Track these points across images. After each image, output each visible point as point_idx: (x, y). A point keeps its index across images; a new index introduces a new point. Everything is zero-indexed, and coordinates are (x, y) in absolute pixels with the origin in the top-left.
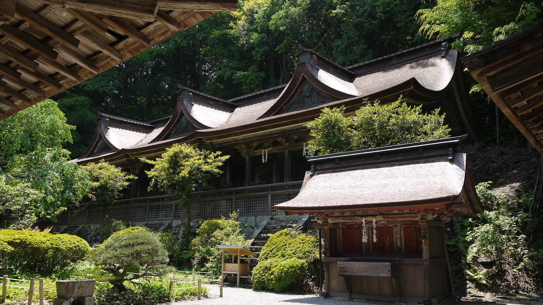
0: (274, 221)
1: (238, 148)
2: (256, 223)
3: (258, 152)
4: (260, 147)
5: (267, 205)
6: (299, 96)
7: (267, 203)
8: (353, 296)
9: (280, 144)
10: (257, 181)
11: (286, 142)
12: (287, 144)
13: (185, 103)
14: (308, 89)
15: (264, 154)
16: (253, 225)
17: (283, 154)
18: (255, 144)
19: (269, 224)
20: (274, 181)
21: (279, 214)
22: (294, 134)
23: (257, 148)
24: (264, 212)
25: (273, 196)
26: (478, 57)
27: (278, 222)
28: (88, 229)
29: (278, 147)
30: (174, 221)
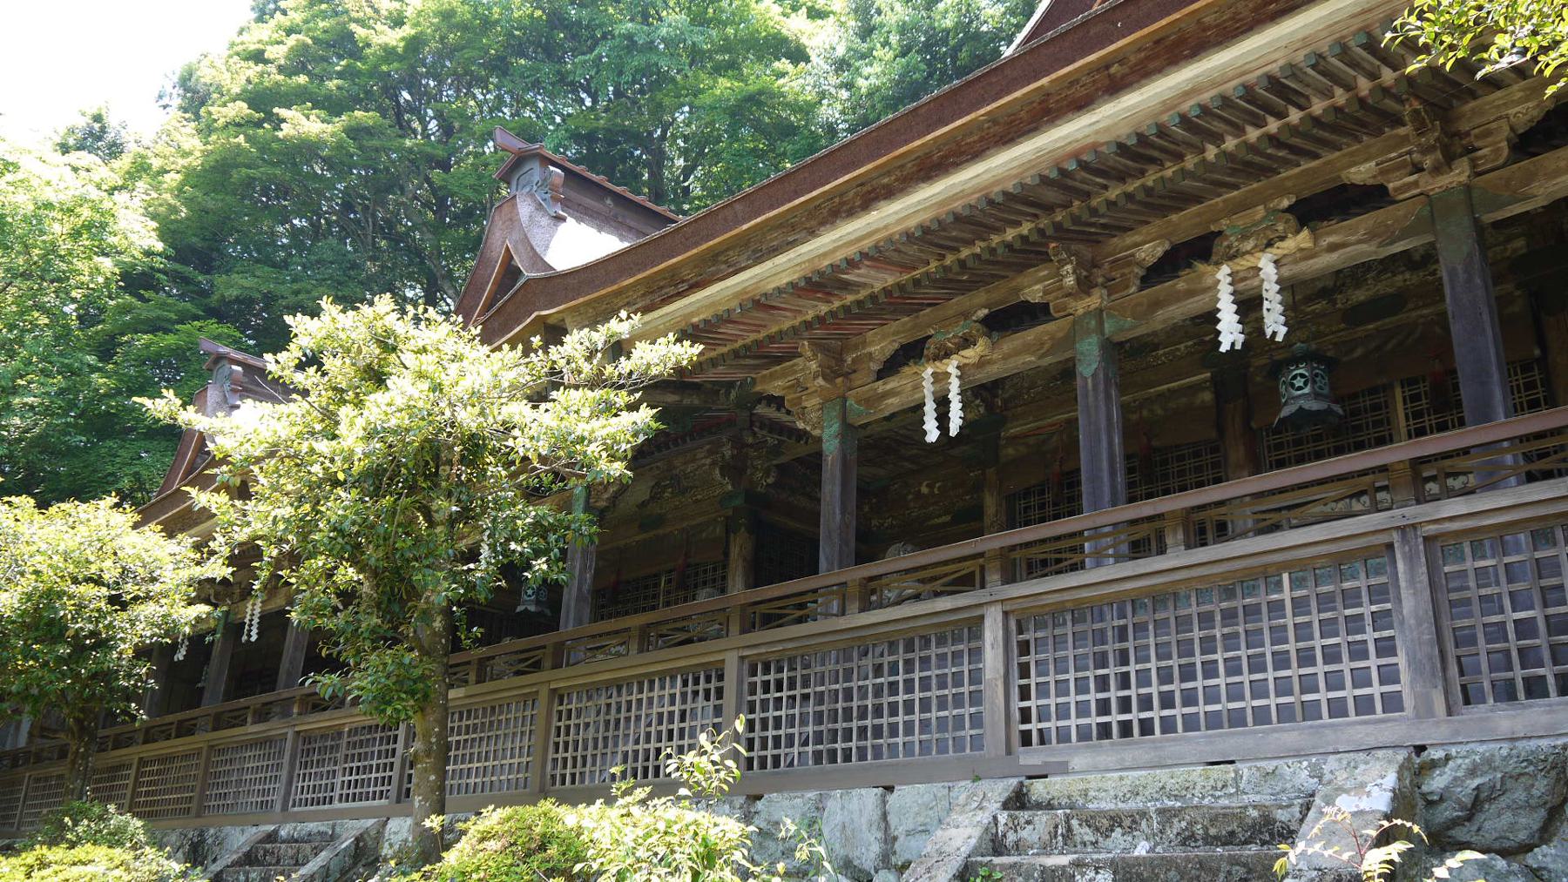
0: (1042, 819)
2: (889, 840)
3: (896, 392)
5: (976, 698)
7: (976, 677)
11: (1085, 285)
12: (1095, 300)
13: (524, 209)
15: (939, 395)
18: (880, 345)
19: (997, 846)
21: (1077, 762)
23: (891, 366)
24: (951, 755)
25: (1019, 620)
27: (1084, 833)
29: (1031, 335)
30: (393, 825)
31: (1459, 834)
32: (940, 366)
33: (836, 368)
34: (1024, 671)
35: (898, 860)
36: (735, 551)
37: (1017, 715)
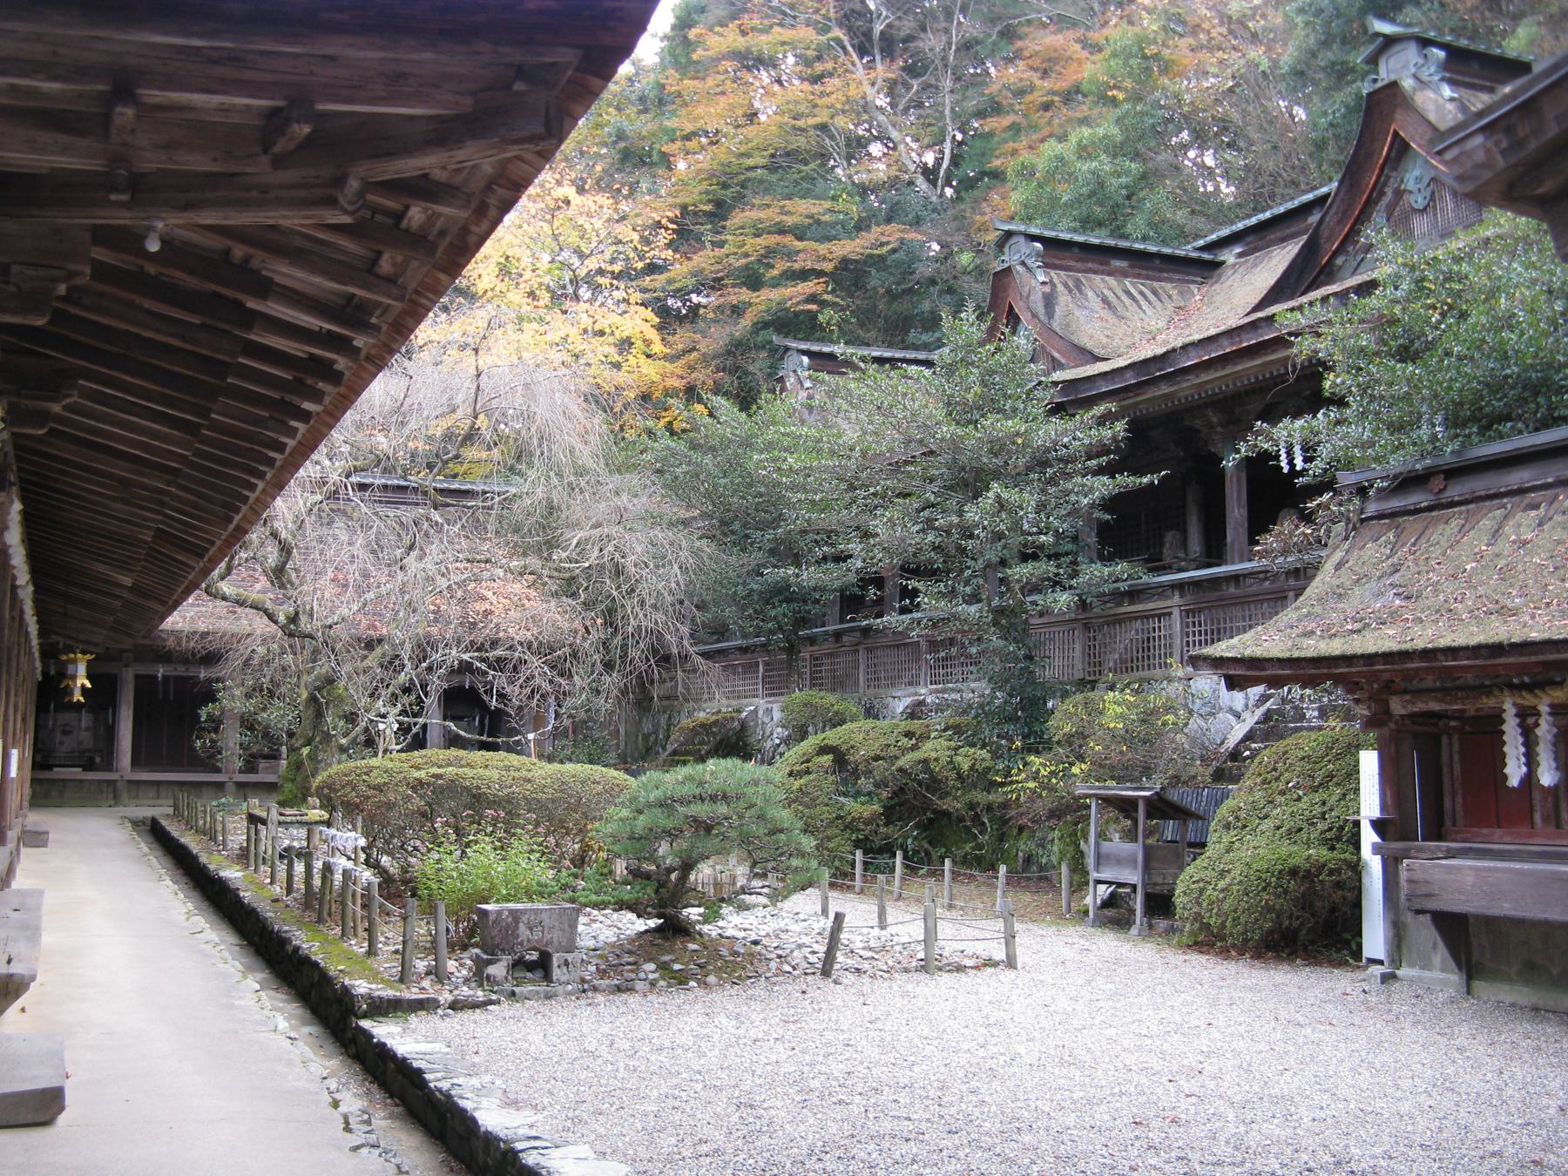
8: (1478, 985)
14: (1418, 180)
26: (1482, 129)
28: (766, 720)
36: (1190, 498)
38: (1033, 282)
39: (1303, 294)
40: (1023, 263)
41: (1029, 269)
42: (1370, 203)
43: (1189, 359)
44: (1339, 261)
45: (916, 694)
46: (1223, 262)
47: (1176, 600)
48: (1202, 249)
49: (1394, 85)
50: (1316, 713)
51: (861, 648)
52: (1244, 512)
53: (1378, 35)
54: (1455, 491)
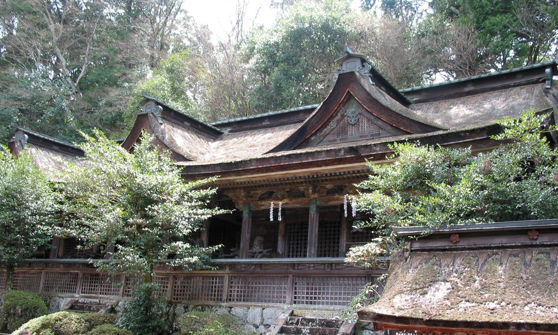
1: (230, 195)
4: (270, 196)
6: (338, 122)
9: (303, 195)
10: (257, 249)
11: (314, 192)
12: (316, 196)
14: (353, 113)
15: (274, 207)
16: (258, 322)
17: (306, 211)
18: (260, 192)
20: (280, 250)
22: (326, 180)
23: (262, 198)
29: (300, 200)
31: (367, 327)
32: (277, 202)
33: (248, 196)
34: (296, 289)
35: (264, 323)
37: (293, 297)
38: (157, 123)
39: (294, 149)
40: (152, 113)
41: (155, 117)
42: (332, 117)
43: (251, 166)
44: (313, 138)
45: (73, 297)
46: (223, 133)
47: (227, 270)
48: (213, 126)
49: (352, 73)
50: (308, 331)
51: (43, 271)
52: (249, 235)
53: (347, 52)
54: (464, 243)
